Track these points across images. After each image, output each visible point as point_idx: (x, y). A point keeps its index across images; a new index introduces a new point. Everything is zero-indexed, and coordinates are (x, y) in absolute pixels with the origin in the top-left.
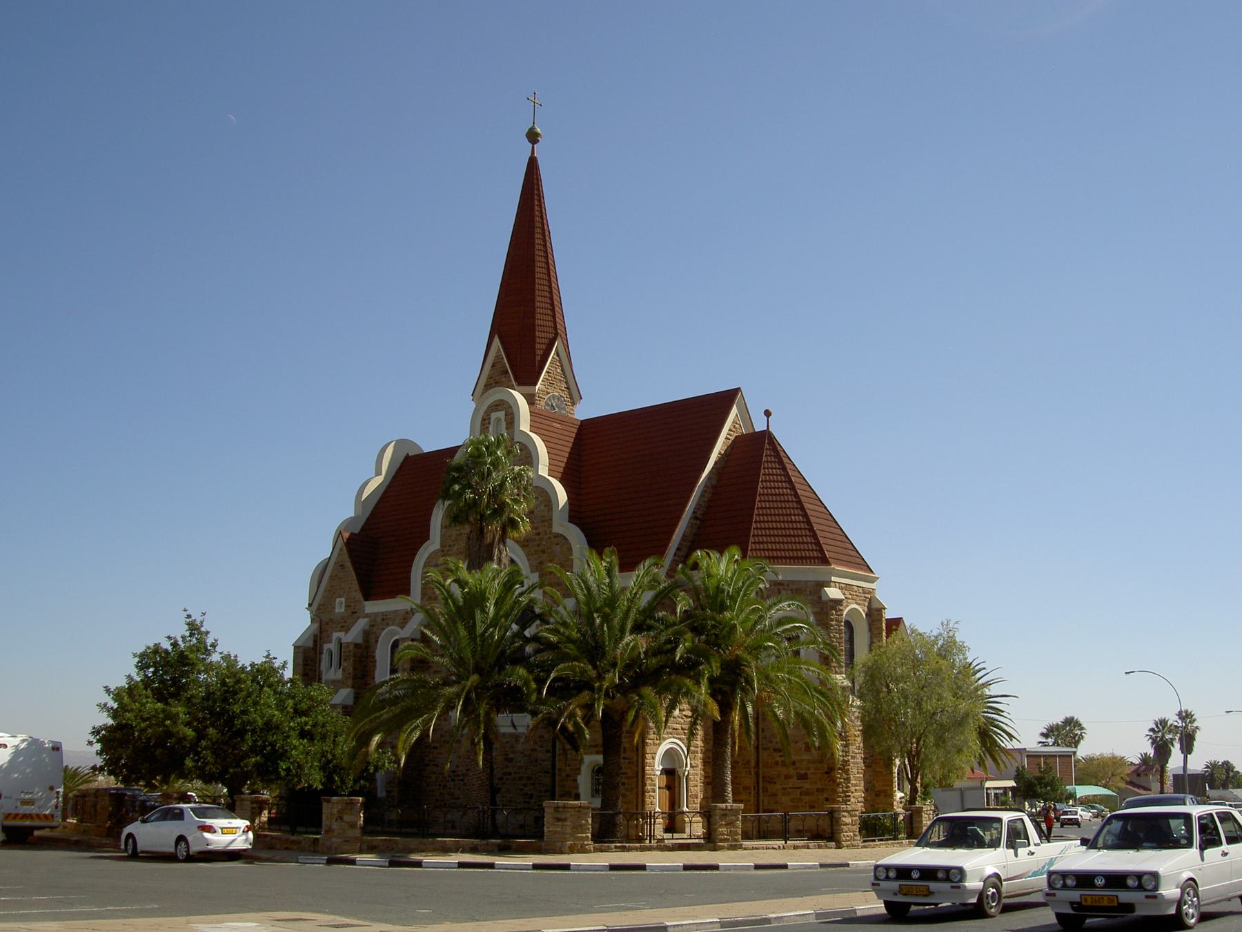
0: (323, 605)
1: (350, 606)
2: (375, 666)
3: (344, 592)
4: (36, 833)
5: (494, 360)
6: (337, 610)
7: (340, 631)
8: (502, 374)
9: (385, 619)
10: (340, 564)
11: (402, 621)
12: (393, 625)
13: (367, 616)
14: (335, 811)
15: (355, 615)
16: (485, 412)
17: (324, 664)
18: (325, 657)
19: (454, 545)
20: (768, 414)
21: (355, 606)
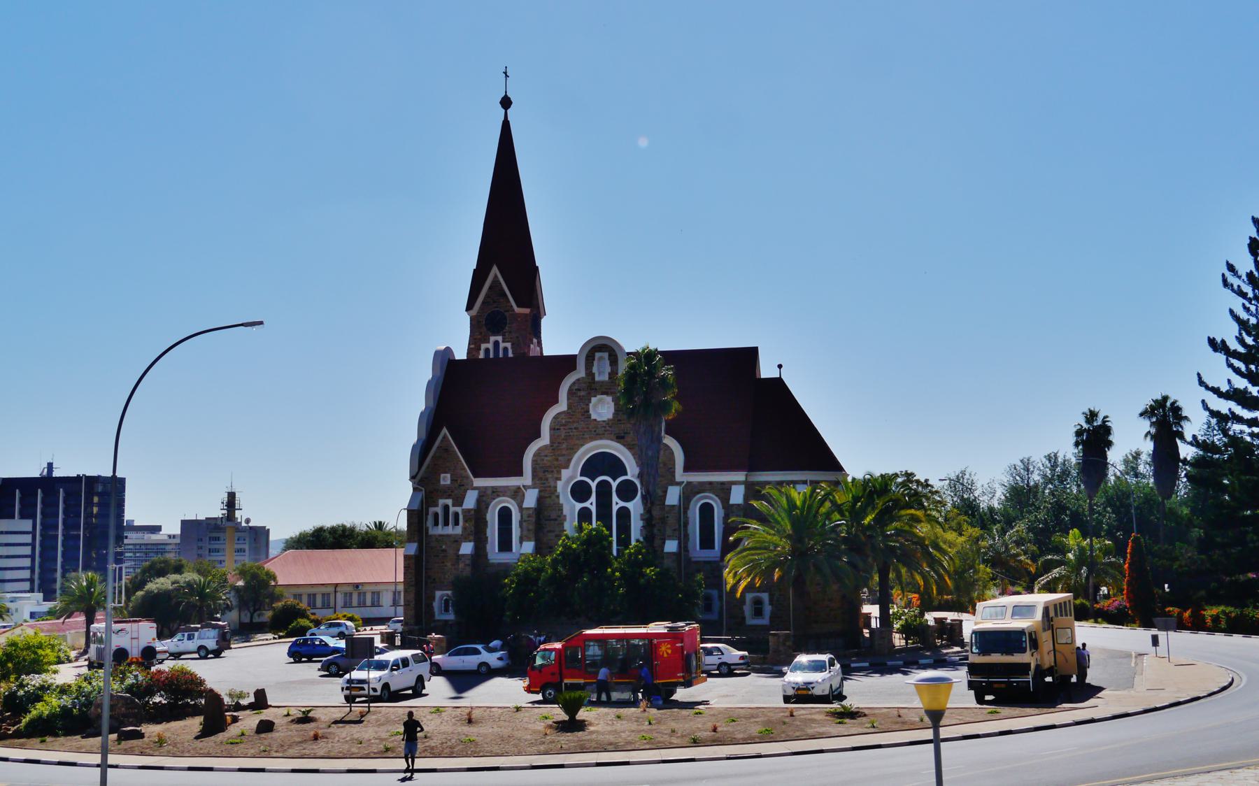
1: (457, 480)
4: (867, 664)
6: (442, 483)
7: (446, 498)
9: (496, 492)
12: (504, 496)
14: (781, 640)
15: (463, 488)
16: (589, 351)
20: (780, 366)
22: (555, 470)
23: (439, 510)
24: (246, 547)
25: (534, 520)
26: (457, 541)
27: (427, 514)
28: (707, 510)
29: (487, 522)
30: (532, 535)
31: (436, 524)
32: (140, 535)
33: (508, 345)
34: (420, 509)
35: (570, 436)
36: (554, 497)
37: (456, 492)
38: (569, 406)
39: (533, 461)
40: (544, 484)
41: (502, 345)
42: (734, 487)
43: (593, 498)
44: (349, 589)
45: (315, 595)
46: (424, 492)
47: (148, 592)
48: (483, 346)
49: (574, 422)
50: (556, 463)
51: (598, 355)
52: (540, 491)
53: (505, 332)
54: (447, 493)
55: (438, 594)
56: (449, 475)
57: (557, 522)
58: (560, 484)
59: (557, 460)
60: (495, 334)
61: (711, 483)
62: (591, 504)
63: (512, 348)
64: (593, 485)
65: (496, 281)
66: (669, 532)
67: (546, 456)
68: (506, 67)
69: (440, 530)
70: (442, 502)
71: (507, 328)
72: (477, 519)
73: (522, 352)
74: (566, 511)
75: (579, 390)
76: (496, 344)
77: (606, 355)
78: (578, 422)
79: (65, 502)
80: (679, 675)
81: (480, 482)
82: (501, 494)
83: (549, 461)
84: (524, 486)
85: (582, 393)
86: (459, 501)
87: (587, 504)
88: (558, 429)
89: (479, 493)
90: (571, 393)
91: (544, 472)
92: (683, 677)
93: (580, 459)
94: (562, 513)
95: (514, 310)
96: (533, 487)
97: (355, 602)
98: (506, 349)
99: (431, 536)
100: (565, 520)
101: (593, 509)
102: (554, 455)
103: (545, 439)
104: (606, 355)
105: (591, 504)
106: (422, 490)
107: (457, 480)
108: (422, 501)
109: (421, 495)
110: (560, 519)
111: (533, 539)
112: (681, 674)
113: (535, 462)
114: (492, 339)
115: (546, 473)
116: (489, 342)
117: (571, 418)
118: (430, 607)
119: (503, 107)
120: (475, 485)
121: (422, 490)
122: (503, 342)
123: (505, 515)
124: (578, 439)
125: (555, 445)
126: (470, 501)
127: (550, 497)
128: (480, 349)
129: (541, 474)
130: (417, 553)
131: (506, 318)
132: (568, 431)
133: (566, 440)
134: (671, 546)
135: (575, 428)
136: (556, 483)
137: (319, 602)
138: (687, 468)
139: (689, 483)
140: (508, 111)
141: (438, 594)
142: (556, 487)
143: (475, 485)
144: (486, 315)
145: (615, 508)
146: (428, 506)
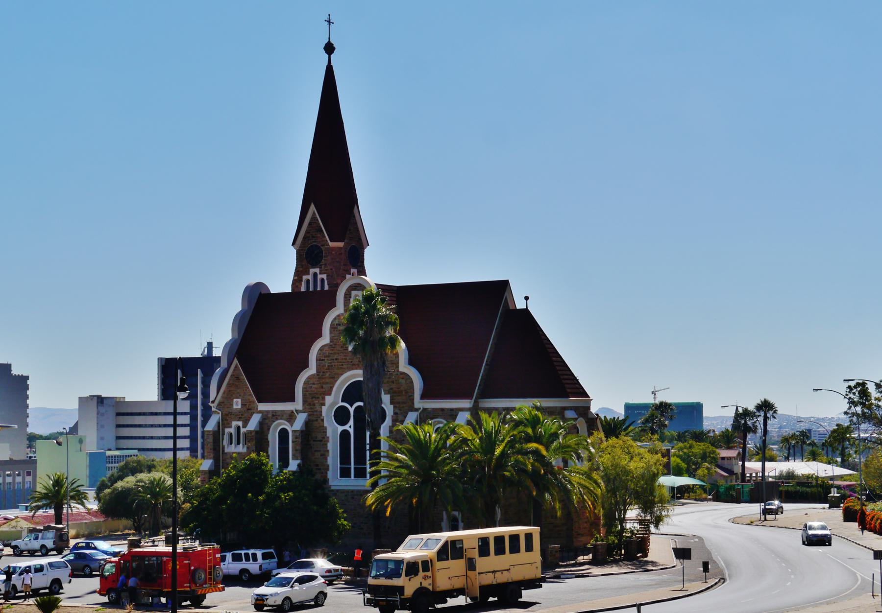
0: (223, 403)
1: (246, 405)
2: (268, 445)
3: (240, 395)
5: (311, 220)
6: (235, 407)
7: (238, 421)
8: (318, 232)
9: (276, 415)
10: (235, 376)
11: (288, 417)
12: (281, 419)
13: (260, 412)
15: (250, 411)
16: (347, 290)
17: (226, 442)
18: (226, 437)
19: (327, 372)
20: (527, 298)
21: (250, 405)
22: (321, 397)
23: (232, 430)
25: (300, 440)
27: (223, 434)
29: (268, 442)
30: (298, 455)
33: (324, 276)
34: (216, 429)
35: (332, 366)
36: (319, 420)
37: (246, 415)
38: (332, 340)
39: (304, 388)
40: (311, 408)
41: (319, 276)
43: (351, 422)
46: (220, 415)
48: (305, 278)
49: (335, 353)
50: (321, 390)
51: (354, 293)
52: (309, 415)
53: (322, 265)
56: (239, 400)
57: (322, 443)
58: (324, 409)
59: (322, 387)
60: (314, 266)
61: (442, 410)
62: (350, 427)
63: (327, 279)
64: (351, 410)
67: (314, 384)
68: (329, 15)
70: (235, 423)
71: (323, 261)
72: (259, 440)
73: (335, 282)
74: (329, 433)
75: (339, 325)
76: (315, 275)
78: (338, 354)
80: (185, 585)
81: (263, 407)
82: (279, 418)
83: (316, 388)
84: (296, 411)
87: (346, 427)
88: (323, 360)
89: (262, 416)
90: (333, 327)
91: (312, 398)
92: (190, 587)
94: (326, 435)
95: (328, 245)
98: (322, 280)
99: (226, 453)
100: (329, 442)
101: (352, 431)
102: (320, 383)
105: (350, 427)
106: (219, 413)
107: (246, 405)
108: (219, 423)
109: (218, 417)
110: (324, 440)
111: (299, 458)
112: (188, 585)
113: (305, 390)
114: (312, 271)
115: (313, 399)
116: (309, 274)
117: (332, 350)
119: (326, 52)
120: (259, 410)
121: (219, 413)
122: (320, 274)
123: (283, 434)
124: (338, 369)
125: (321, 374)
126: (253, 424)
127: (317, 420)
128: (302, 281)
129: (309, 400)
130: (213, 468)
131: (322, 252)
132: (330, 362)
133: (329, 369)
135: (336, 359)
136: (321, 408)
138: (423, 397)
139: (425, 409)
140: (331, 56)
142: (321, 412)
143: (259, 410)
144: (307, 249)
146: (224, 426)
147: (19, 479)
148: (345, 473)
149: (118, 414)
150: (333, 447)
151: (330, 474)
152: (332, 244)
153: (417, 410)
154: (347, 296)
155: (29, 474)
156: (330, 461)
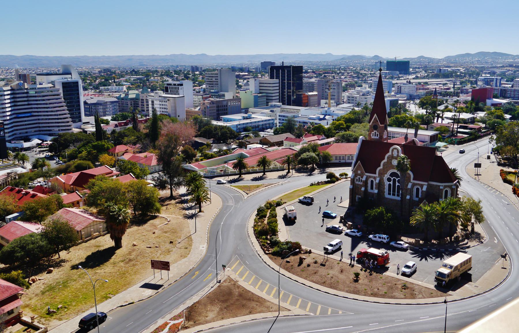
9: (370, 177)
18: (356, 180)
23: (358, 178)
24: (336, 88)
26: (361, 186)
28: (418, 190)
31: (357, 181)
32: (307, 79)
33: (378, 133)
38: (387, 161)
41: (377, 133)
42: (424, 186)
43: (392, 182)
44: (349, 155)
45: (340, 157)
47: (301, 158)
48: (372, 133)
51: (394, 150)
54: (359, 175)
55: (357, 196)
56: (360, 171)
58: (384, 178)
61: (419, 184)
64: (392, 179)
65: (376, 118)
66: (408, 193)
69: (357, 183)
70: (358, 177)
72: (366, 182)
74: (385, 184)
76: (375, 132)
77: (396, 150)
79: (287, 73)
81: (367, 174)
85: (390, 158)
86: (362, 177)
87: (390, 183)
90: (388, 158)
93: (389, 173)
96: (378, 177)
97: (350, 158)
98: (377, 134)
103: (381, 167)
104: (396, 150)
105: (391, 183)
110: (384, 185)
113: (379, 172)
114: (374, 131)
115: (381, 174)
118: (355, 199)
123: (372, 182)
126: (364, 179)
134: (408, 197)
137: (342, 159)
138: (414, 179)
141: (357, 196)
145: (397, 185)
147: (237, 103)
148: (389, 194)
149: (260, 83)
150: (387, 187)
151: (385, 194)
152: (380, 125)
153: (412, 183)
154: (393, 151)
155: (239, 102)
156: (385, 190)
